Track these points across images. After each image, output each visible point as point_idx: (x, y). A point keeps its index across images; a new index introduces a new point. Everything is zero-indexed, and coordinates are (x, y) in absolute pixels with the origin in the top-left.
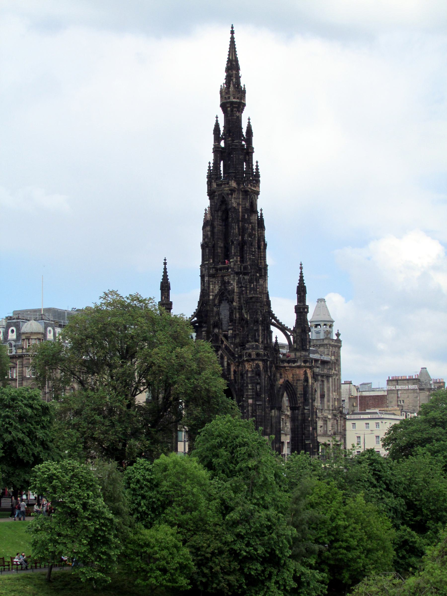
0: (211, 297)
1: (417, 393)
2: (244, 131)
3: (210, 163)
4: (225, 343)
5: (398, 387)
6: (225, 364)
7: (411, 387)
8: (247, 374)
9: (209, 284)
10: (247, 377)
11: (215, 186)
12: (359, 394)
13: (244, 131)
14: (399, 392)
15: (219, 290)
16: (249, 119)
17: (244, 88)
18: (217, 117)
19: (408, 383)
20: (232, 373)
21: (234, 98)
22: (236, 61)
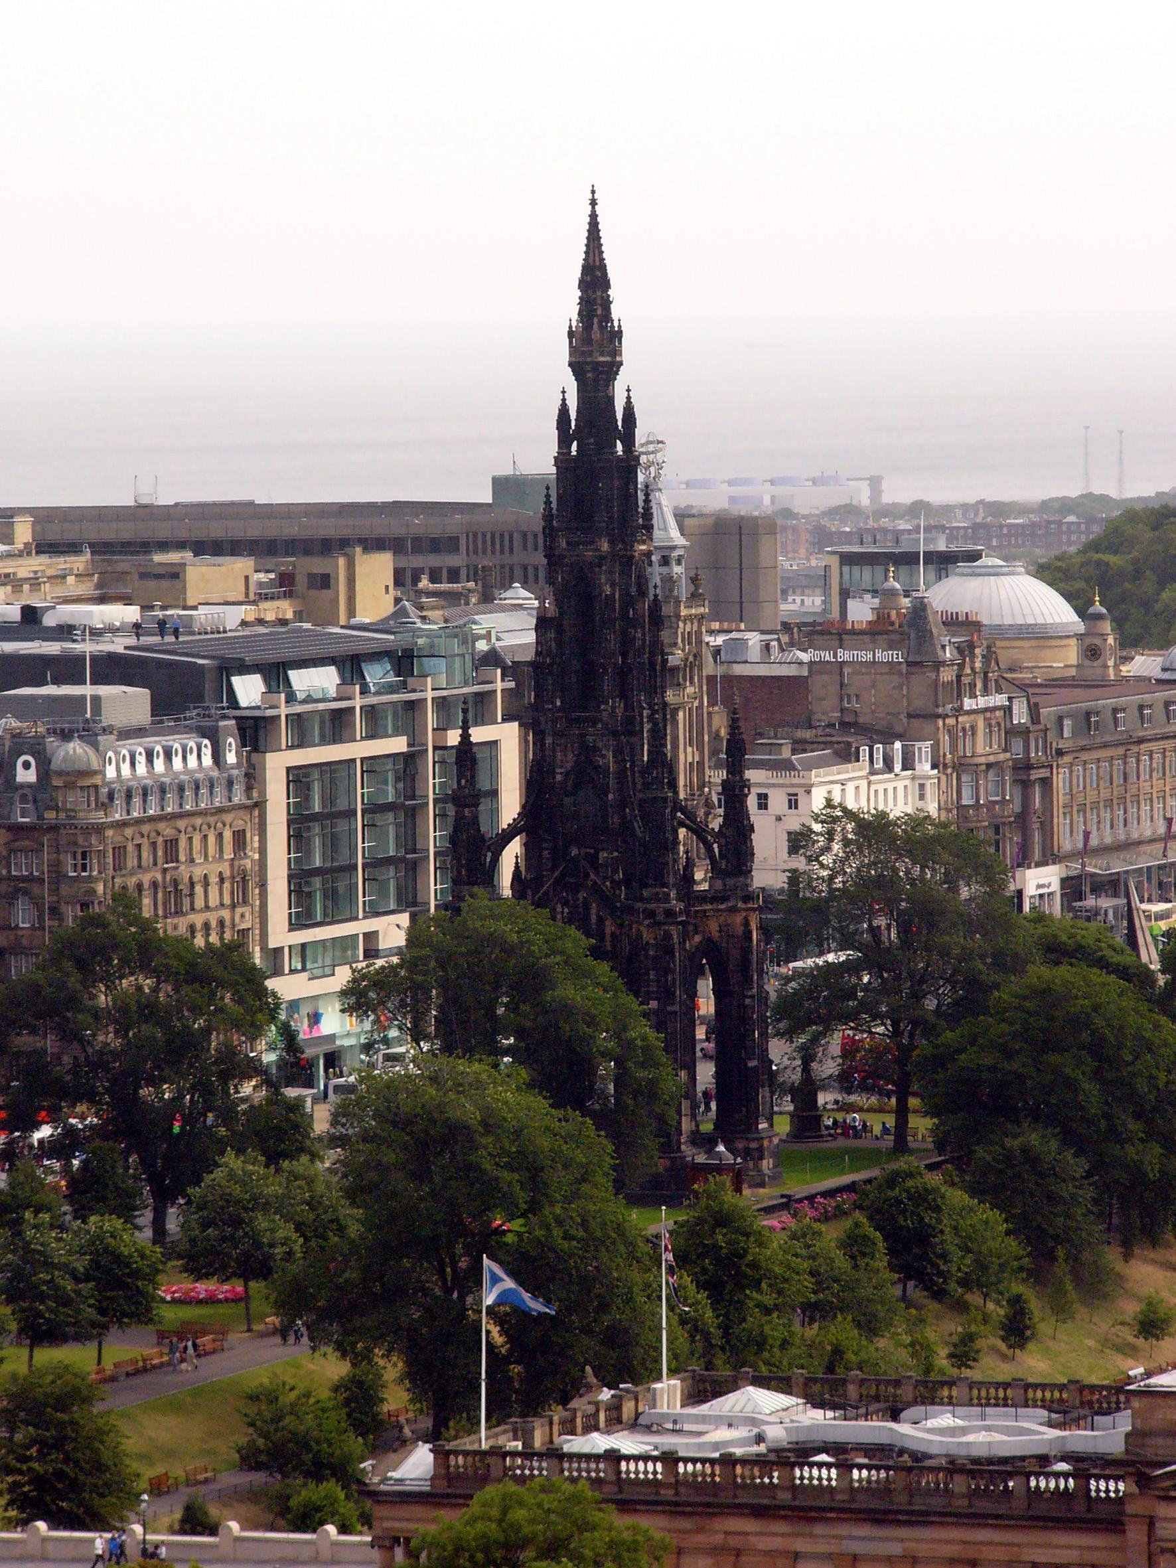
0: (559, 778)
1: (900, 673)
2: (619, 416)
3: (548, 488)
4: (592, 876)
5: (844, 655)
6: (594, 918)
7: (882, 656)
8: (646, 951)
9: (554, 751)
10: (647, 956)
11: (564, 545)
12: (720, 671)
13: (619, 416)
14: (846, 670)
15: (576, 762)
16: (628, 390)
17: (620, 326)
18: (563, 392)
19: (873, 642)
20: (608, 937)
21: (602, 355)
22: (603, 268)
